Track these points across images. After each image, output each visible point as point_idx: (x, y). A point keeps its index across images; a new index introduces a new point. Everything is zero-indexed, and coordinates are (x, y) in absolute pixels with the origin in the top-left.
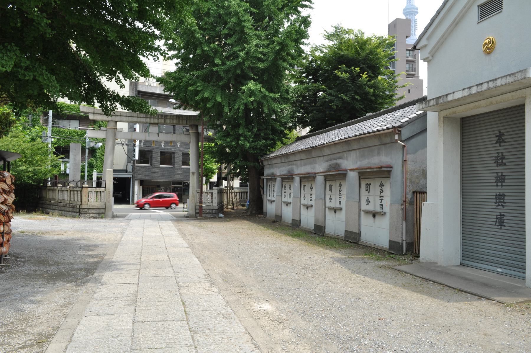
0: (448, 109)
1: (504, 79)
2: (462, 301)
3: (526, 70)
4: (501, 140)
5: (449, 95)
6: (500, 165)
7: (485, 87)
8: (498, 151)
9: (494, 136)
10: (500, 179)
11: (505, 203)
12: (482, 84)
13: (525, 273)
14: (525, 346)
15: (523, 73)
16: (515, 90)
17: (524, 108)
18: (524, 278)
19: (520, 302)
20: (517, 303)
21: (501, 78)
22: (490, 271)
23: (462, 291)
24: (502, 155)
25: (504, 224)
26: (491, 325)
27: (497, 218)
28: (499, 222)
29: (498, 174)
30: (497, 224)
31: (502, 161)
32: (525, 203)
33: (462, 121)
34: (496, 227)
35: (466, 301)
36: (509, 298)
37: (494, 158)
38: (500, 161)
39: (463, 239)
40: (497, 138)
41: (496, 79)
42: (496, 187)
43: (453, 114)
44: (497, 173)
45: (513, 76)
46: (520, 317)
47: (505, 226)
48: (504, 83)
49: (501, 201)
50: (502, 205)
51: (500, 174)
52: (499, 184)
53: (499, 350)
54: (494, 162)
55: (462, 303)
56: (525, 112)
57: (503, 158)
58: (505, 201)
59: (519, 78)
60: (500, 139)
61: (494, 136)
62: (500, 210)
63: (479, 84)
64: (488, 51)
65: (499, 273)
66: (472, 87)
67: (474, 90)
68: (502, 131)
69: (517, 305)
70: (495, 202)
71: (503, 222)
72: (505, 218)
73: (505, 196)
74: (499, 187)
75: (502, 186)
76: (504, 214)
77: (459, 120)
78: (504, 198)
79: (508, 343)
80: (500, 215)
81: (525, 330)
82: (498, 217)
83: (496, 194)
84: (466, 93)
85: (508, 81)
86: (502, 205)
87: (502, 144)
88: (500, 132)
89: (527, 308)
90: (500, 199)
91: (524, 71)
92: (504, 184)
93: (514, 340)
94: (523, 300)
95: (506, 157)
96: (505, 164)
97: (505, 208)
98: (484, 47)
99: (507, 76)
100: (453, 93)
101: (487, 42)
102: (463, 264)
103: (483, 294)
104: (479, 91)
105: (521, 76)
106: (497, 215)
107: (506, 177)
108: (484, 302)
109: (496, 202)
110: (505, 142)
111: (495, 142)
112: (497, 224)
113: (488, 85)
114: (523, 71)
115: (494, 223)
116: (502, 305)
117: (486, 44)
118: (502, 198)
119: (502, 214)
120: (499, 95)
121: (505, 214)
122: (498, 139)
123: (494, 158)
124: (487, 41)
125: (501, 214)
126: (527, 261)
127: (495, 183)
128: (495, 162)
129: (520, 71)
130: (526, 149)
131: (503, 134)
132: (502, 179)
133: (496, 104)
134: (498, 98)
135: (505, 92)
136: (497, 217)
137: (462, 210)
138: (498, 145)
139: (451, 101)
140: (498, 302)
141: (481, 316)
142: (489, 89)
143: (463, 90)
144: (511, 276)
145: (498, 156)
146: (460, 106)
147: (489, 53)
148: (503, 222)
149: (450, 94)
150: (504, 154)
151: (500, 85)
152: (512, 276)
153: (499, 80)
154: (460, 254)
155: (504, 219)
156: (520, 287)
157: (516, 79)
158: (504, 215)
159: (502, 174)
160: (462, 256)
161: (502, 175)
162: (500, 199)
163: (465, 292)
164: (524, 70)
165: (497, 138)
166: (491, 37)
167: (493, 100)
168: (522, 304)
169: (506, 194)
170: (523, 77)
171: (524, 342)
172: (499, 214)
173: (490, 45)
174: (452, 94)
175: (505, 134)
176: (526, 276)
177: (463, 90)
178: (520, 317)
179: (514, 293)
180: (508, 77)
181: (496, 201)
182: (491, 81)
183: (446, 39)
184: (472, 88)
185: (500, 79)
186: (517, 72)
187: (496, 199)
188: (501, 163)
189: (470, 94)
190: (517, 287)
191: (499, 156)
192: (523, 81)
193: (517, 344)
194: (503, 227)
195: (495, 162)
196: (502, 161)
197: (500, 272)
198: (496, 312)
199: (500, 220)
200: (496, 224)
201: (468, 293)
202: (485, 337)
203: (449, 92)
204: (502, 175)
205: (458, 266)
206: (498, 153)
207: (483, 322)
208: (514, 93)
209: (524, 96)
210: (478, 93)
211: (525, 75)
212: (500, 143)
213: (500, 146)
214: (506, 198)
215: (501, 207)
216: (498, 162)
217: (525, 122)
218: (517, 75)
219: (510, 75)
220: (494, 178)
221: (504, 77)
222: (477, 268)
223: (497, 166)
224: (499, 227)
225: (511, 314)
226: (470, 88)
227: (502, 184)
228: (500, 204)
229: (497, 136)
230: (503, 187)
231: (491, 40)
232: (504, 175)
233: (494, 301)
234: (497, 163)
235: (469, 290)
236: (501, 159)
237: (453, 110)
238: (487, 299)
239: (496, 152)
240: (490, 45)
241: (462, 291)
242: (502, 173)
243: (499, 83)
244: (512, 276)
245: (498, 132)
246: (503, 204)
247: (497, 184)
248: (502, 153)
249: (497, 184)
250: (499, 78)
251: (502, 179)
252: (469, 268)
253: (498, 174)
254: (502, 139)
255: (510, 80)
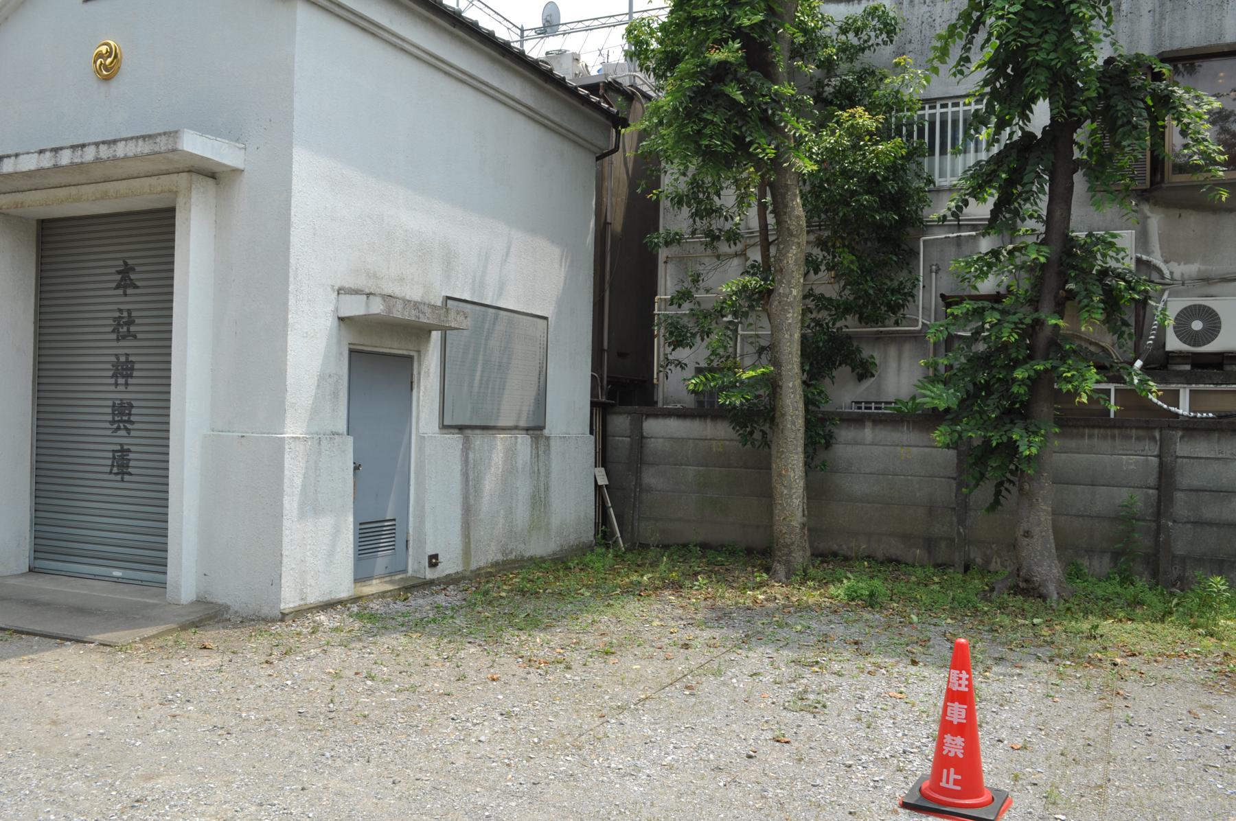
0: (5, 193)
1: (131, 144)
2: (15, 656)
3: (176, 132)
4: (128, 282)
5: (5, 159)
6: (124, 338)
7: (90, 154)
8: (122, 307)
9: (113, 270)
10: (123, 369)
11: (132, 423)
12: (83, 146)
13: (165, 573)
14: (137, 728)
15: (171, 139)
16: (156, 173)
17: (174, 217)
18: (163, 585)
19: (149, 637)
20: (143, 640)
21: (126, 140)
22: (97, 577)
23: (22, 632)
24: (130, 316)
25: (130, 470)
26: (73, 699)
27: (114, 458)
28: (118, 466)
29: (118, 359)
30: (115, 470)
31: (128, 329)
32: (168, 423)
33: (42, 229)
34: (112, 477)
35: (24, 655)
36: (126, 632)
37: (111, 322)
38: (125, 329)
39: (38, 508)
40: (119, 277)
41: (115, 142)
42: (113, 388)
43: (17, 207)
44: (116, 355)
45: (151, 141)
46: (142, 668)
47: (130, 474)
48: (130, 154)
49: (125, 418)
50: (126, 429)
51: (123, 359)
52: (121, 381)
53: (78, 749)
54: (110, 329)
55: (13, 661)
56: (174, 225)
57: (131, 322)
58: (133, 418)
59: (163, 148)
60: (125, 279)
61: (113, 270)
62: (121, 439)
63: (78, 146)
64: (105, 73)
65: (116, 580)
66: (61, 149)
67: (65, 158)
68: (130, 262)
69: (141, 646)
70: (110, 422)
71: (128, 467)
72: (131, 456)
73: (132, 407)
74: (122, 388)
75: (127, 384)
76: (130, 447)
77: (35, 223)
78: (130, 411)
79: (102, 731)
80: (122, 451)
81: (146, 694)
82: (116, 454)
83: (114, 403)
84: (47, 161)
85: (139, 150)
86: (126, 429)
87: (129, 291)
88: (126, 264)
89: (161, 647)
90: (122, 414)
91: (173, 134)
92: (130, 381)
93: (117, 722)
94: (155, 633)
95: (137, 321)
96: (135, 337)
97: (133, 433)
98: (95, 62)
99: (137, 138)
100: (17, 155)
101: (104, 52)
102: (36, 570)
103: (69, 632)
104: (76, 161)
105: (166, 144)
106: (114, 451)
107: (136, 366)
108: (70, 650)
109: (113, 422)
110: (136, 287)
111: (114, 285)
112: (115, 470)
113: (98, 152)
114: (170, 133)
115: (108, 469)
116: (109, 649)
117: (100, 55)
118: (127, 412)
119: (125, 447)
120: (124, 179)
121: (133, 448)
122: (122, 280)
123: (111, 322)
124: (104, 49)
125: (122, 448)
126: (170, 548)
127: (112, 377)
128: (113, 331)
129: (165, 134)
130: (175, 305)
131: (133, 269)
132: (127, 369)
133: (116, 198)
134: (122, 186)
135: (136, 175)
136: (114, 455)
137: (37, 440)
138: (120, 292)
139: (10, 174)
140: (101, 644)
141: (55, 682)
142: (98, 160)
143: (41, 152)
144: (141, 583)
145: (120, 317)
146: (36, 189)
147: (107, 79)
148: (128, 467)
149: (9, 156)
150: (134, 314)
151: (122, 155)
152: (144, 583)
153: (121, 145)
154: (28, 547)
155: (129, 460)
156: (154, 606)
157: (157, 149)
158: (129, 451)
159: (127, 359)
160: (35, 551)
161: (127, 361)
162: (122, 412)
163: (28, 633)
164: (173, 132)
165: (119, 277)
166: (112, 43)
167: (111, 187)
168: (153, 641)
169: (135, 404)
170: (170, 147)
171: (138, 721)
172: (118, 448)
173: (109, 60)
174: (13, 158)
175: (138, 269)
176: (168, 578)
177: (41, 152)
178: (142, 668)
179: (139, 619)
180: (140, 142)
181: (113, 418)
182: (104, 143)
183: (7, 18)
184: (60, 152)
185: (123, 142)
186: (160, 134)
187: (113, 414)
188: (126, 334)
189: (56, 166)
190: (147, 606)
191: (123, 318)
192: (170, 156)
193: (122, 727)
194: (127, 478)
195: (113, 331)
196: (128, 329)
197: (118, 578)
198: (92, 667)
199: (121, 463)
200: (111, 470)
201: (35, 634)
202: (54, 728)
203: (9, 152)
204: (127, 361)
205: (23, 575)
206: (120, 310)
207: (55, 694)
208: (153, 180)
209: (175, 189)
210: (73, 165)
211: (176, 143)
212: (125, 287)
213: (125, 295)
214: (134, 411)
215: (123, 433)
216: (121, 330)
217: (173, 248)
218: (158, 140)
219: (144, 137)
220: (109, 366)
221: (132, 138)
222: (68, 574)
223: (118, 340)
224: (119, 477)
225: (123, 667)
226: (56, 150)
227: (126, 381)
228: (121, 425)
229: (119, 272)
230: (130, 388)
231: (111, 48)
232: (131, 361)
233: (92, 643)
234: (119, 332)
235: (38, 628)
236: (126, 323)
237: (19, 197)
238: (78, 641)
239: (115, 307)
240: (109, 60)
241: (22, 632)
242: (127, 355)
243: (121, 150)
244: (144, 583)
245: (121, 263)
246: (129, 426)
247: (116, 381)
248: (129, 310)
249: (116, 381)
250: (121, 140)
251: (127, 369)
252: (48, 577)
253: (118, 359)
254: (131, 280)
255: (143, 148)
